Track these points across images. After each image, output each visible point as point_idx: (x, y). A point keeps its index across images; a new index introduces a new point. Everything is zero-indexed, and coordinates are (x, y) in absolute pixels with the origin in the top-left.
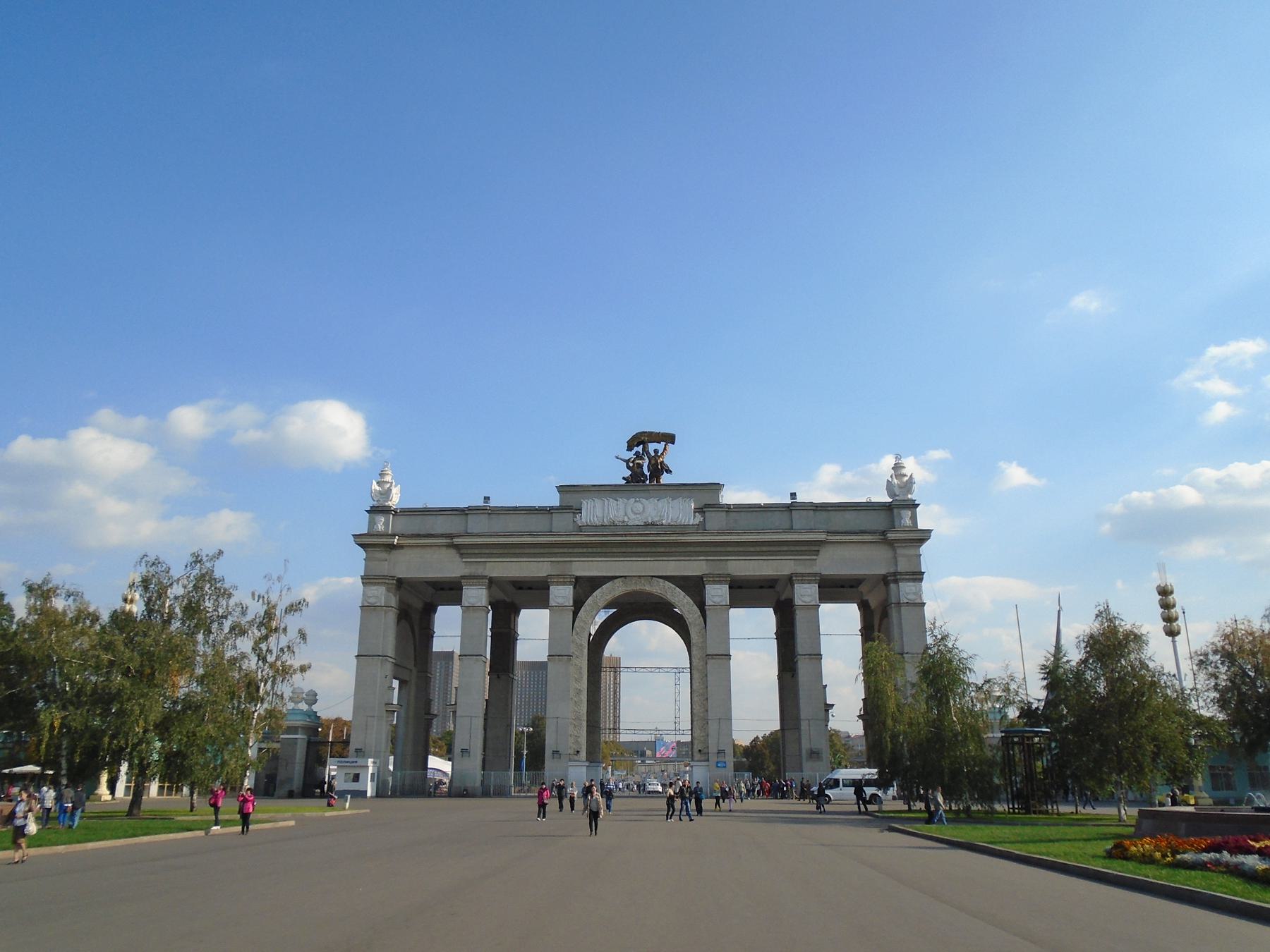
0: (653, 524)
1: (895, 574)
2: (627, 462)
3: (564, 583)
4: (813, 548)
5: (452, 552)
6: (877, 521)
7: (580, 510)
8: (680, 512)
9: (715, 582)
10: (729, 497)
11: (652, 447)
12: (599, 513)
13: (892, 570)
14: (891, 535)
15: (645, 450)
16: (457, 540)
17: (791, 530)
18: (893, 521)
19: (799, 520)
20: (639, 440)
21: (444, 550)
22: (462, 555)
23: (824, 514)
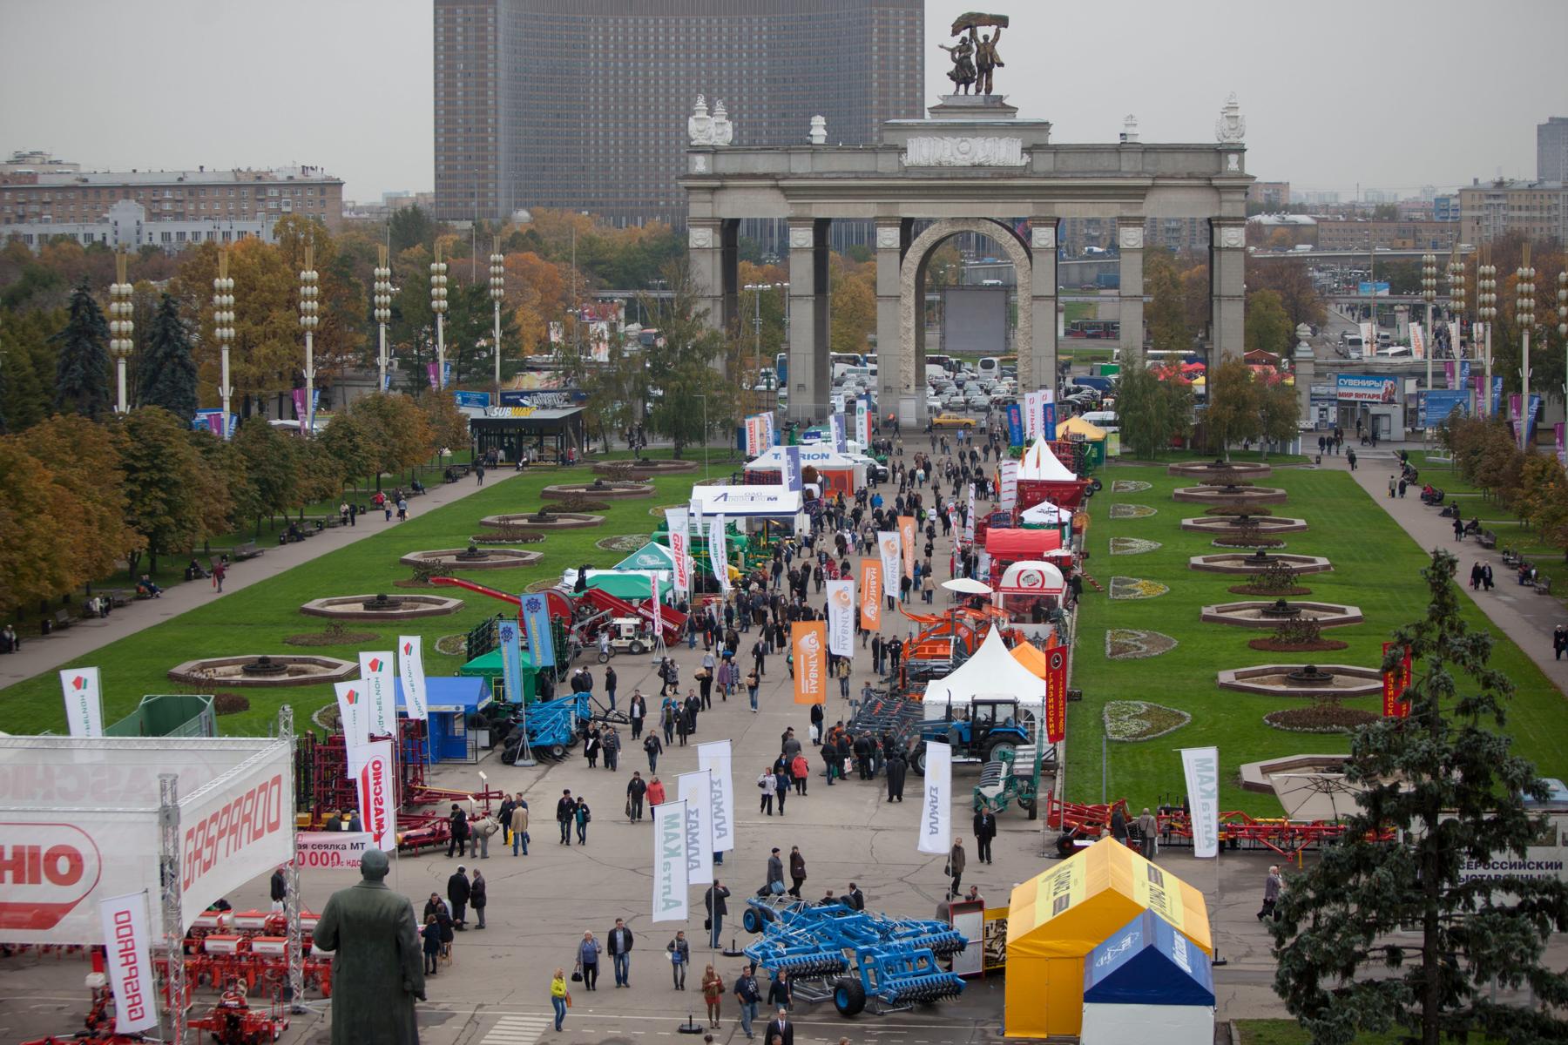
0: (980, 166)
1: (1219, 218)
2: (953, 51)
3: (891, 225)
4: (1140, 192)
5: (776, 194)
6: (1206, 164)
7: (904, 150)
8: (1005, 152)
9: (1041, 225)
10: (1053, 139)
11: (982, 31)
12: (925, 152)
13: (1217, 214)
14: (1215, 182)
15: (973, 34)
16: (781, 183)
17: (1117, 173)
18: (1220, 165)
19: (1128, 163)
20: (968, 22)
21: (768, 191)
22: (787, 197)
23: (1153, 156)
